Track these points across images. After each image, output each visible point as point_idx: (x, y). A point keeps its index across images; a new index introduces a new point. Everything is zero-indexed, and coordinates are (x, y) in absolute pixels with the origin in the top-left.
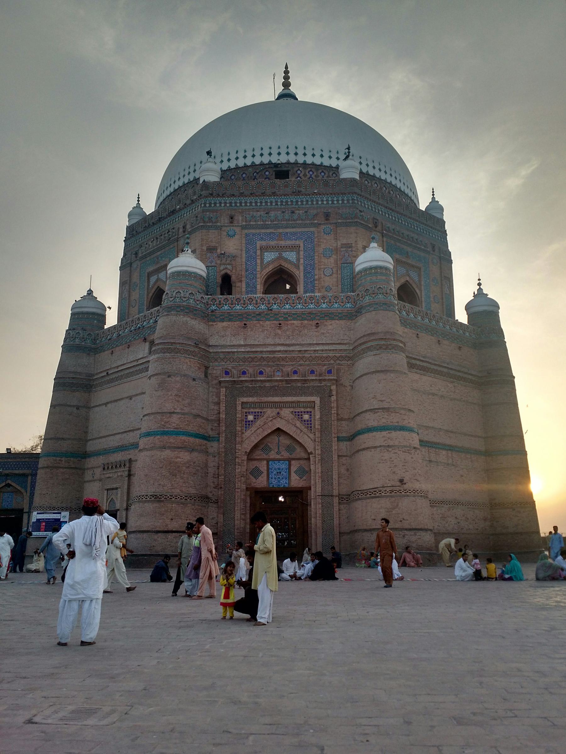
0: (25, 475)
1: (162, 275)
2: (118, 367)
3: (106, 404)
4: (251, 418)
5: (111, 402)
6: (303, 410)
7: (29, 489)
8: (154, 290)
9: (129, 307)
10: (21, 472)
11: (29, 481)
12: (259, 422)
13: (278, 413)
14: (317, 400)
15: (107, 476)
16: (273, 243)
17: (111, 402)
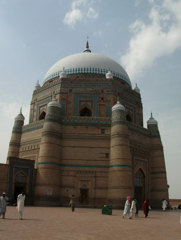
0: (27, 169)
1: (89, 104)
2: (80, 134)
3: (74, 147)
4: (136, 164)
5: (76, 147)
6: (144, 163)
7: (29, 175)
8: (83, 107)
9: (66, 109)
10: (26, 167)
11: (29, 172)
12: (137, 166)
13: (140, 164)
14: (147, 160)
15: (81, 175)
16: (128, 106)
17: (76, 147)
